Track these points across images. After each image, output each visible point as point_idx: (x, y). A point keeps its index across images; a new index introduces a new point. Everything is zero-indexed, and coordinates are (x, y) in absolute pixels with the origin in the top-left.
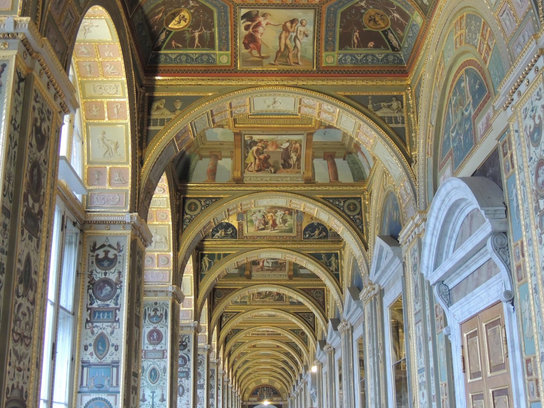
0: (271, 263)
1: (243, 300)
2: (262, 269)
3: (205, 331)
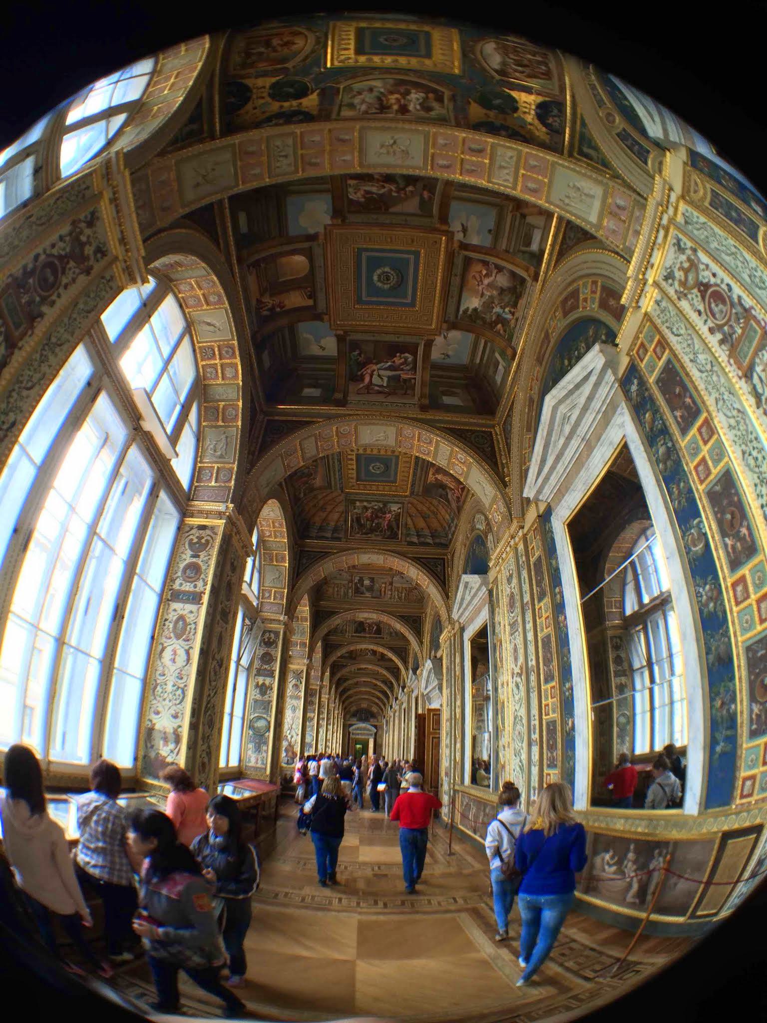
0: (386, 379)
1: (336, 535)
2: (369, 388)
3: (230, 480)
